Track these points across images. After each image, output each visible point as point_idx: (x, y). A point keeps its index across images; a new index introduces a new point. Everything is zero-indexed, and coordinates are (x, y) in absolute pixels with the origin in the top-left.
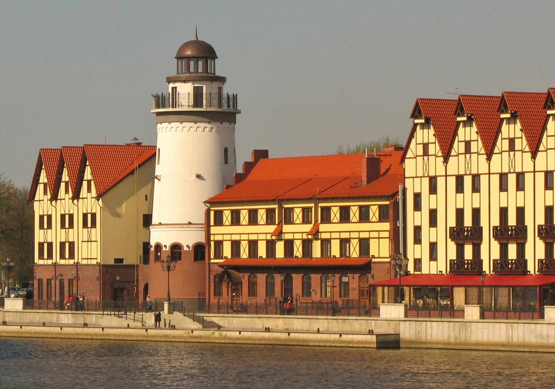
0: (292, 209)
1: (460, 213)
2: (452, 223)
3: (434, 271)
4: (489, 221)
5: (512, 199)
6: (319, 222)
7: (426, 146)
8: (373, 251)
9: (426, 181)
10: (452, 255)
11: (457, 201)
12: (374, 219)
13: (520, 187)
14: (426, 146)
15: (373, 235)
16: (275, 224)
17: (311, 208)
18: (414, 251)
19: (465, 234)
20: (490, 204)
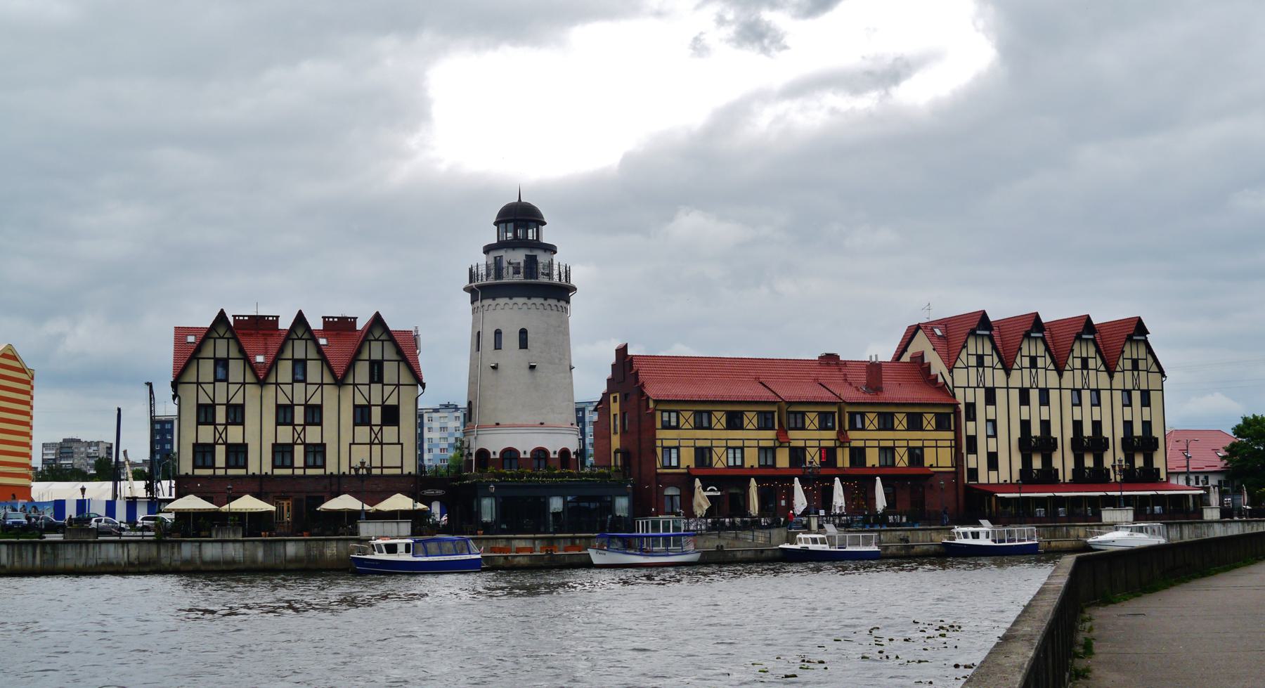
0: (803, 414)
1: (1025, 425)
2: (1016, 433)
3: (993, 480)
4: (1062, 433)
5: (1087, 415)
6: (847, 427)
7: (980, 359)
8: (929, 458)
9: (981, 393)
10: (1018, 464)
11: (1019, 413)
12: (929, 427)
13: (1097, 402)
14: (980, 359)
15: (926, 443)
16: (772, 428)
17: (833, 413)
18: (971, 461)
19: (1036, 444)
20: (1061, 419)
